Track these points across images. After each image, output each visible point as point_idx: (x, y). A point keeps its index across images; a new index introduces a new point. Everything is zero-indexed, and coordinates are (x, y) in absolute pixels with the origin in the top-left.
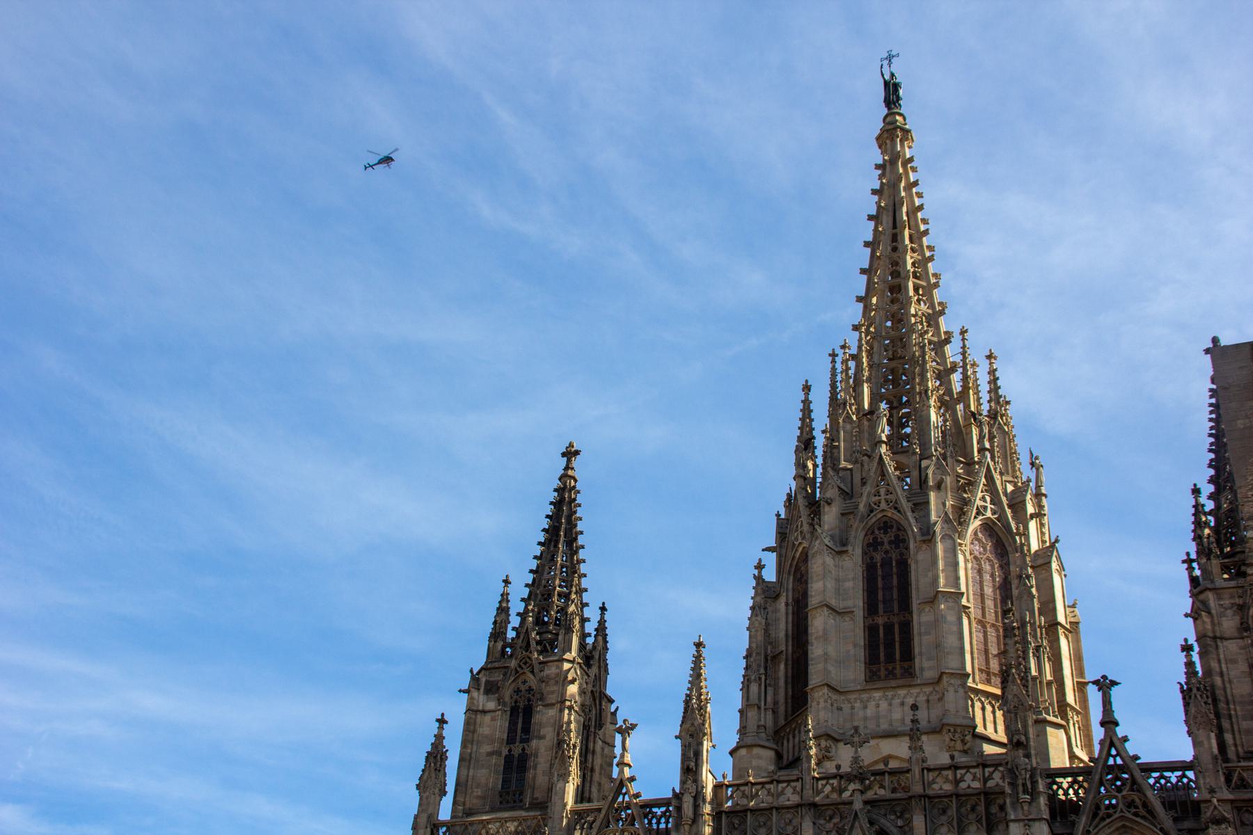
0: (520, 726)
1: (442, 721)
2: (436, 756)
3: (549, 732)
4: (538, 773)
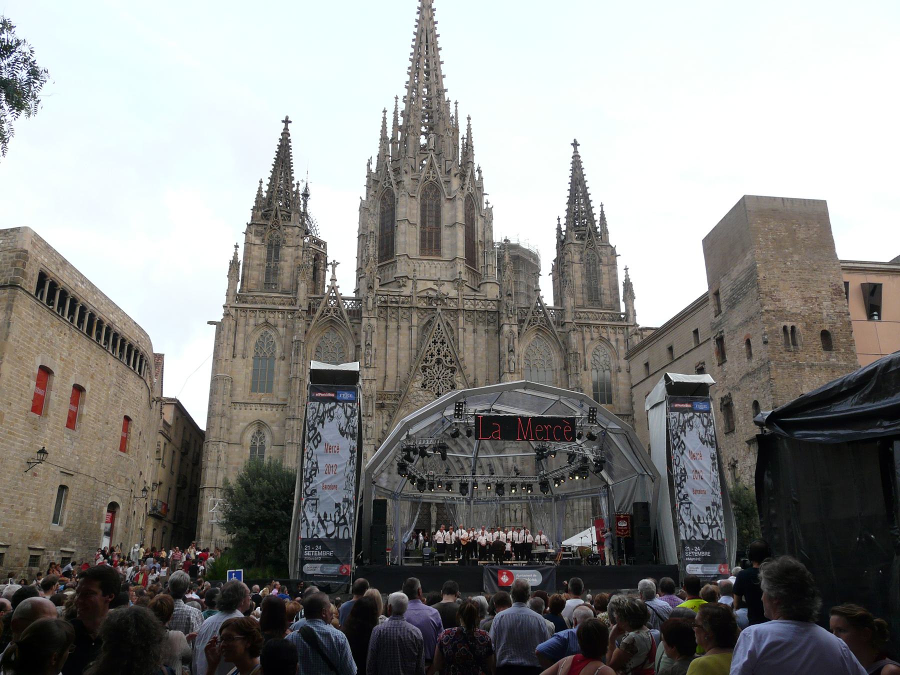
1: (237, 246)
2: (234, 264)
3: (289, 258)
4: (285, 277)
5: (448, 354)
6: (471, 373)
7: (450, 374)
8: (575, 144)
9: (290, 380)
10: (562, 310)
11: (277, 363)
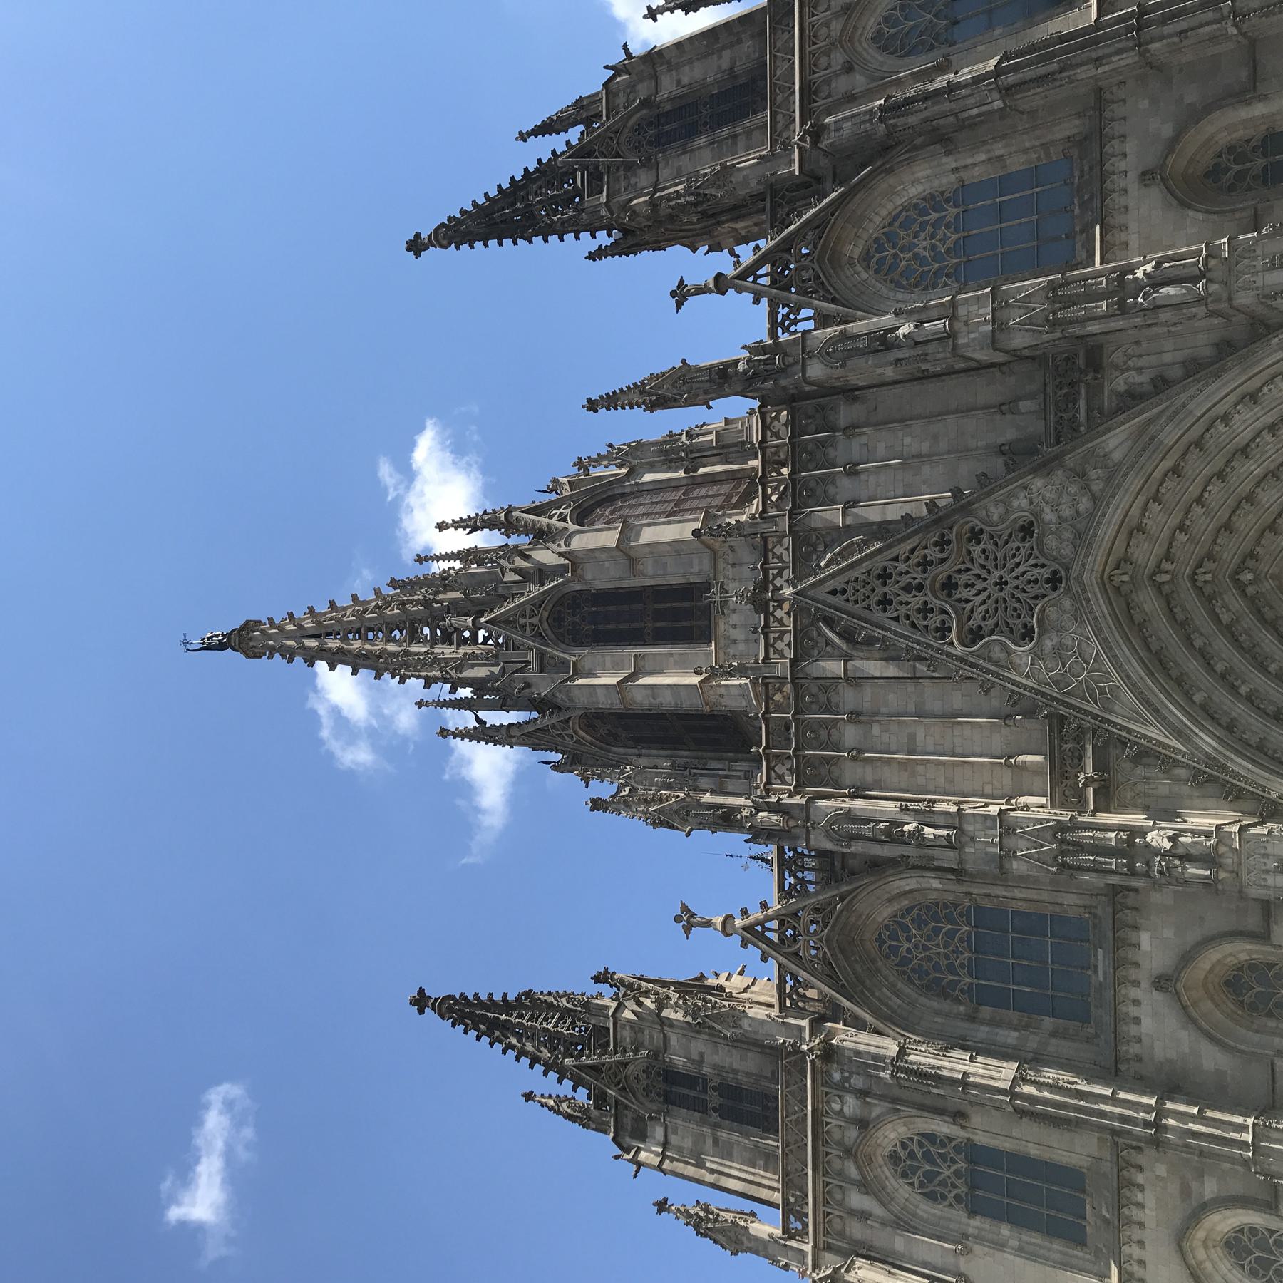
0: (687, 1092)
1: (662, 1206)
3: (699, 1046)
4: (744, 1065)
5: (914, 560)
6: (966, 471)
7: (986, 543)
8: (416, 246)
9: (1022, 1113)
10: (775, 193)
11: (981, 1139)
